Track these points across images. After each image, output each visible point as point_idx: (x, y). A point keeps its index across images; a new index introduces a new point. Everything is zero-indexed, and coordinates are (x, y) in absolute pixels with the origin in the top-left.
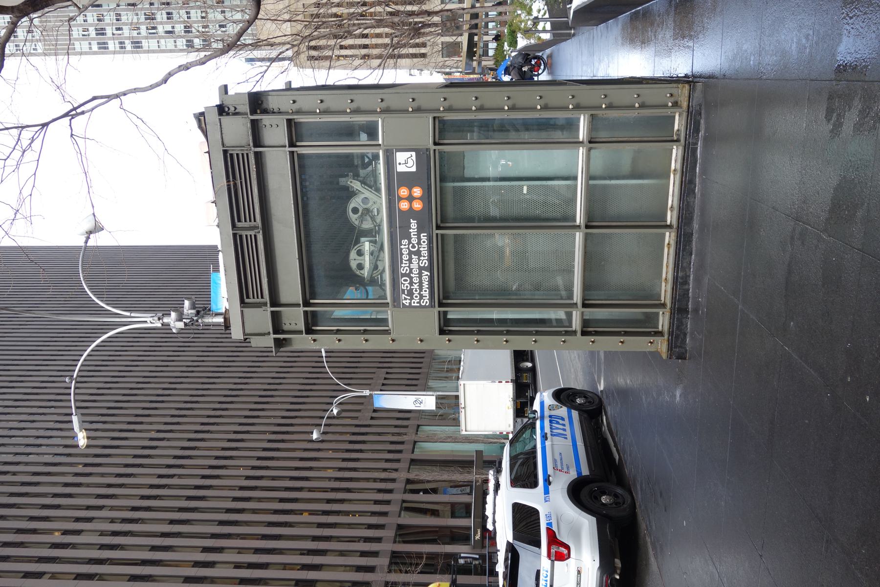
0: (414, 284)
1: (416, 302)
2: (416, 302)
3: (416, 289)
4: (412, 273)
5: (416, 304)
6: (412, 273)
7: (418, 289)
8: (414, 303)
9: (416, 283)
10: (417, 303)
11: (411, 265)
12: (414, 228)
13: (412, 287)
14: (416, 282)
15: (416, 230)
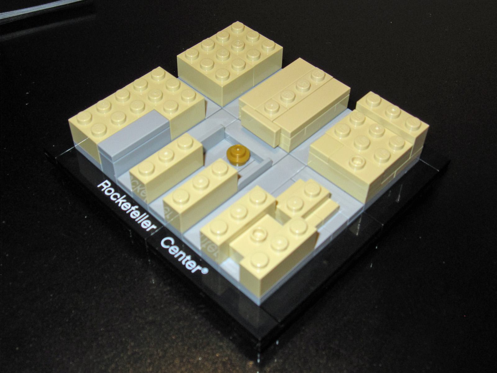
0: (125, 201)
1: (105, 187)
2: (105, 187)
3: (118, 199)
4: (136, 209)
5: (103, 184)
6: (136, 209)
7: (114, 199)
8: (107, 184)
9: (123, 203)
10: (102, 187)
11: (147, 216)
12: (189, 263)
13: (125, 196)
14: (125, 204)
15: (183, 263)
